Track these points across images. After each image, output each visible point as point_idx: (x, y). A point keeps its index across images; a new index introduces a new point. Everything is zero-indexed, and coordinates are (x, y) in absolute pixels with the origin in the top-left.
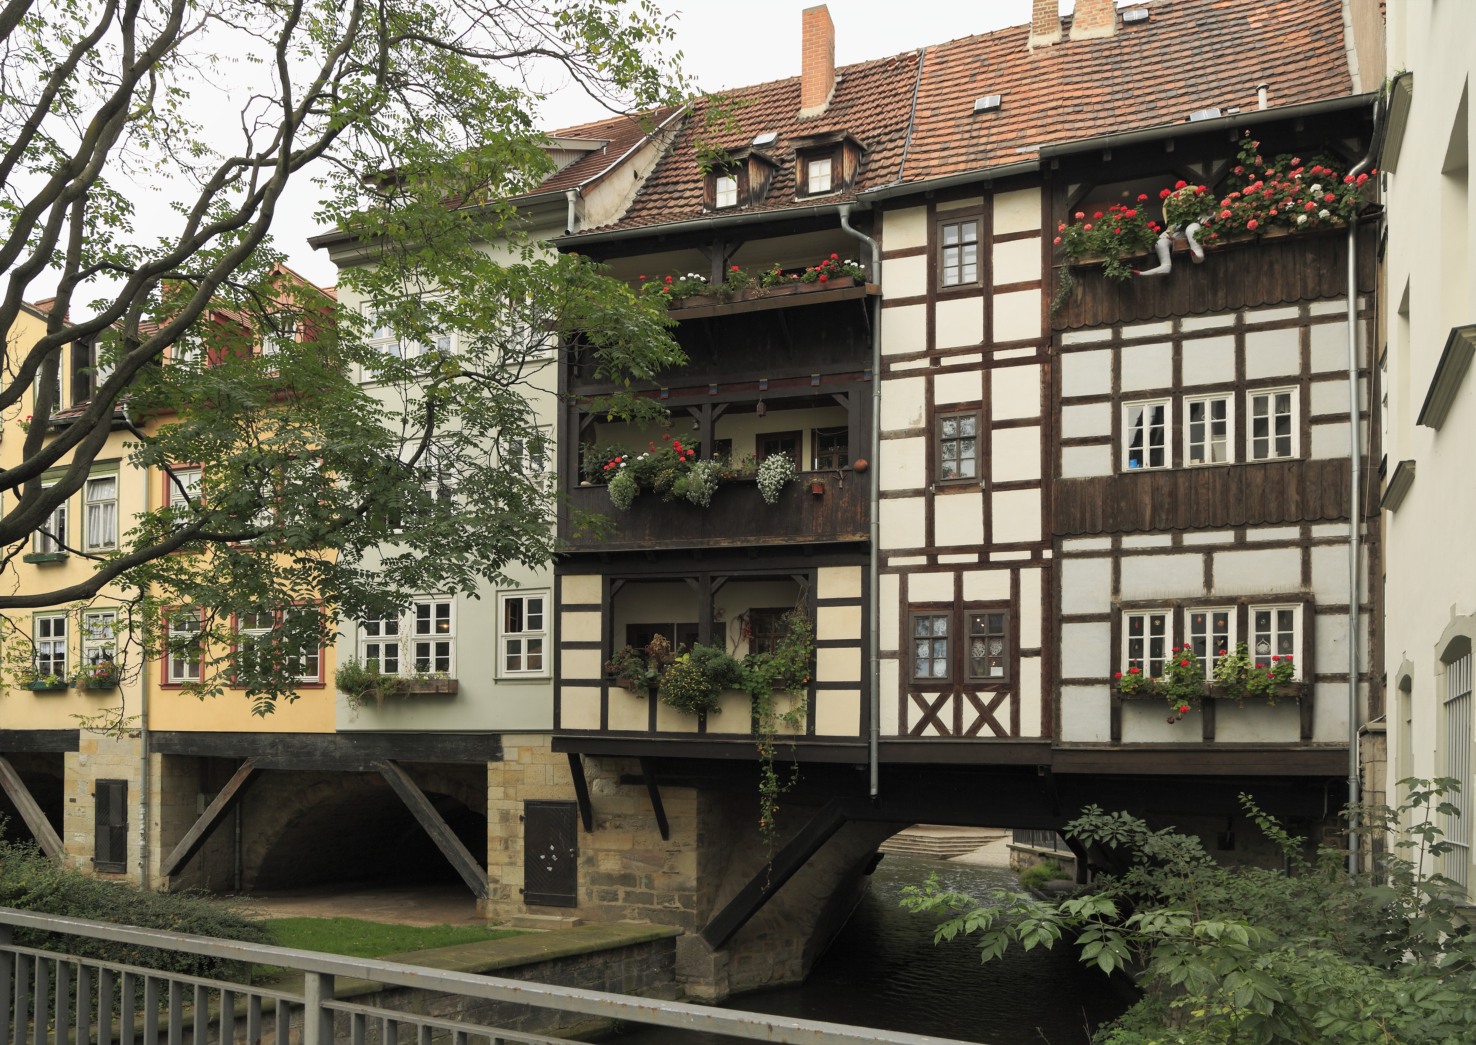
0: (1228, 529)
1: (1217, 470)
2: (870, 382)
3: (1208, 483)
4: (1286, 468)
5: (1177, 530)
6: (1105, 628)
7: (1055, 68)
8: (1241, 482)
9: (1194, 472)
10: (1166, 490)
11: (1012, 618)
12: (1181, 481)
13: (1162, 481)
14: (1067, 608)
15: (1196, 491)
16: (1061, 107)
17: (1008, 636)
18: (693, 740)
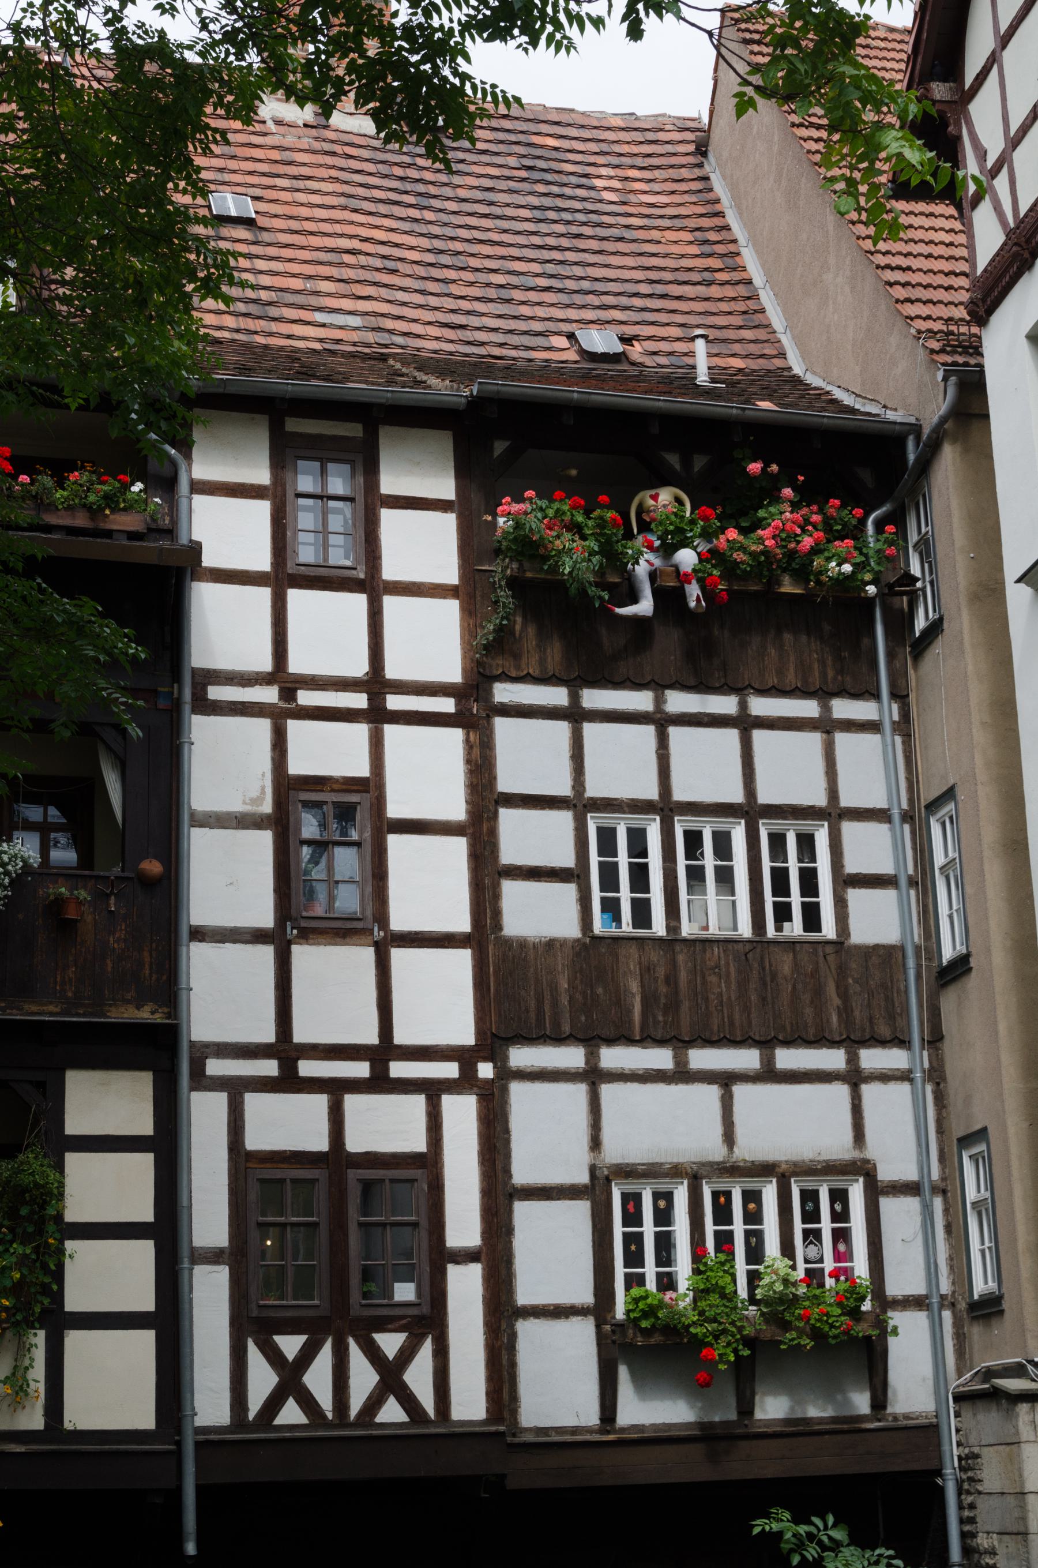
0: (750, 1047)
1: (730, 946)
3: (718, 966)
4: (820, 950)
5: (680, 1043)
6: (581, 1210)
7: (324, 173)
8: (764, 969)
9: (698, 945)
10: (661, 972)
12: (681, 958)
13: (654, 956)
14: (522, 1174)
15: (703, 977)
17: (424, 1223)
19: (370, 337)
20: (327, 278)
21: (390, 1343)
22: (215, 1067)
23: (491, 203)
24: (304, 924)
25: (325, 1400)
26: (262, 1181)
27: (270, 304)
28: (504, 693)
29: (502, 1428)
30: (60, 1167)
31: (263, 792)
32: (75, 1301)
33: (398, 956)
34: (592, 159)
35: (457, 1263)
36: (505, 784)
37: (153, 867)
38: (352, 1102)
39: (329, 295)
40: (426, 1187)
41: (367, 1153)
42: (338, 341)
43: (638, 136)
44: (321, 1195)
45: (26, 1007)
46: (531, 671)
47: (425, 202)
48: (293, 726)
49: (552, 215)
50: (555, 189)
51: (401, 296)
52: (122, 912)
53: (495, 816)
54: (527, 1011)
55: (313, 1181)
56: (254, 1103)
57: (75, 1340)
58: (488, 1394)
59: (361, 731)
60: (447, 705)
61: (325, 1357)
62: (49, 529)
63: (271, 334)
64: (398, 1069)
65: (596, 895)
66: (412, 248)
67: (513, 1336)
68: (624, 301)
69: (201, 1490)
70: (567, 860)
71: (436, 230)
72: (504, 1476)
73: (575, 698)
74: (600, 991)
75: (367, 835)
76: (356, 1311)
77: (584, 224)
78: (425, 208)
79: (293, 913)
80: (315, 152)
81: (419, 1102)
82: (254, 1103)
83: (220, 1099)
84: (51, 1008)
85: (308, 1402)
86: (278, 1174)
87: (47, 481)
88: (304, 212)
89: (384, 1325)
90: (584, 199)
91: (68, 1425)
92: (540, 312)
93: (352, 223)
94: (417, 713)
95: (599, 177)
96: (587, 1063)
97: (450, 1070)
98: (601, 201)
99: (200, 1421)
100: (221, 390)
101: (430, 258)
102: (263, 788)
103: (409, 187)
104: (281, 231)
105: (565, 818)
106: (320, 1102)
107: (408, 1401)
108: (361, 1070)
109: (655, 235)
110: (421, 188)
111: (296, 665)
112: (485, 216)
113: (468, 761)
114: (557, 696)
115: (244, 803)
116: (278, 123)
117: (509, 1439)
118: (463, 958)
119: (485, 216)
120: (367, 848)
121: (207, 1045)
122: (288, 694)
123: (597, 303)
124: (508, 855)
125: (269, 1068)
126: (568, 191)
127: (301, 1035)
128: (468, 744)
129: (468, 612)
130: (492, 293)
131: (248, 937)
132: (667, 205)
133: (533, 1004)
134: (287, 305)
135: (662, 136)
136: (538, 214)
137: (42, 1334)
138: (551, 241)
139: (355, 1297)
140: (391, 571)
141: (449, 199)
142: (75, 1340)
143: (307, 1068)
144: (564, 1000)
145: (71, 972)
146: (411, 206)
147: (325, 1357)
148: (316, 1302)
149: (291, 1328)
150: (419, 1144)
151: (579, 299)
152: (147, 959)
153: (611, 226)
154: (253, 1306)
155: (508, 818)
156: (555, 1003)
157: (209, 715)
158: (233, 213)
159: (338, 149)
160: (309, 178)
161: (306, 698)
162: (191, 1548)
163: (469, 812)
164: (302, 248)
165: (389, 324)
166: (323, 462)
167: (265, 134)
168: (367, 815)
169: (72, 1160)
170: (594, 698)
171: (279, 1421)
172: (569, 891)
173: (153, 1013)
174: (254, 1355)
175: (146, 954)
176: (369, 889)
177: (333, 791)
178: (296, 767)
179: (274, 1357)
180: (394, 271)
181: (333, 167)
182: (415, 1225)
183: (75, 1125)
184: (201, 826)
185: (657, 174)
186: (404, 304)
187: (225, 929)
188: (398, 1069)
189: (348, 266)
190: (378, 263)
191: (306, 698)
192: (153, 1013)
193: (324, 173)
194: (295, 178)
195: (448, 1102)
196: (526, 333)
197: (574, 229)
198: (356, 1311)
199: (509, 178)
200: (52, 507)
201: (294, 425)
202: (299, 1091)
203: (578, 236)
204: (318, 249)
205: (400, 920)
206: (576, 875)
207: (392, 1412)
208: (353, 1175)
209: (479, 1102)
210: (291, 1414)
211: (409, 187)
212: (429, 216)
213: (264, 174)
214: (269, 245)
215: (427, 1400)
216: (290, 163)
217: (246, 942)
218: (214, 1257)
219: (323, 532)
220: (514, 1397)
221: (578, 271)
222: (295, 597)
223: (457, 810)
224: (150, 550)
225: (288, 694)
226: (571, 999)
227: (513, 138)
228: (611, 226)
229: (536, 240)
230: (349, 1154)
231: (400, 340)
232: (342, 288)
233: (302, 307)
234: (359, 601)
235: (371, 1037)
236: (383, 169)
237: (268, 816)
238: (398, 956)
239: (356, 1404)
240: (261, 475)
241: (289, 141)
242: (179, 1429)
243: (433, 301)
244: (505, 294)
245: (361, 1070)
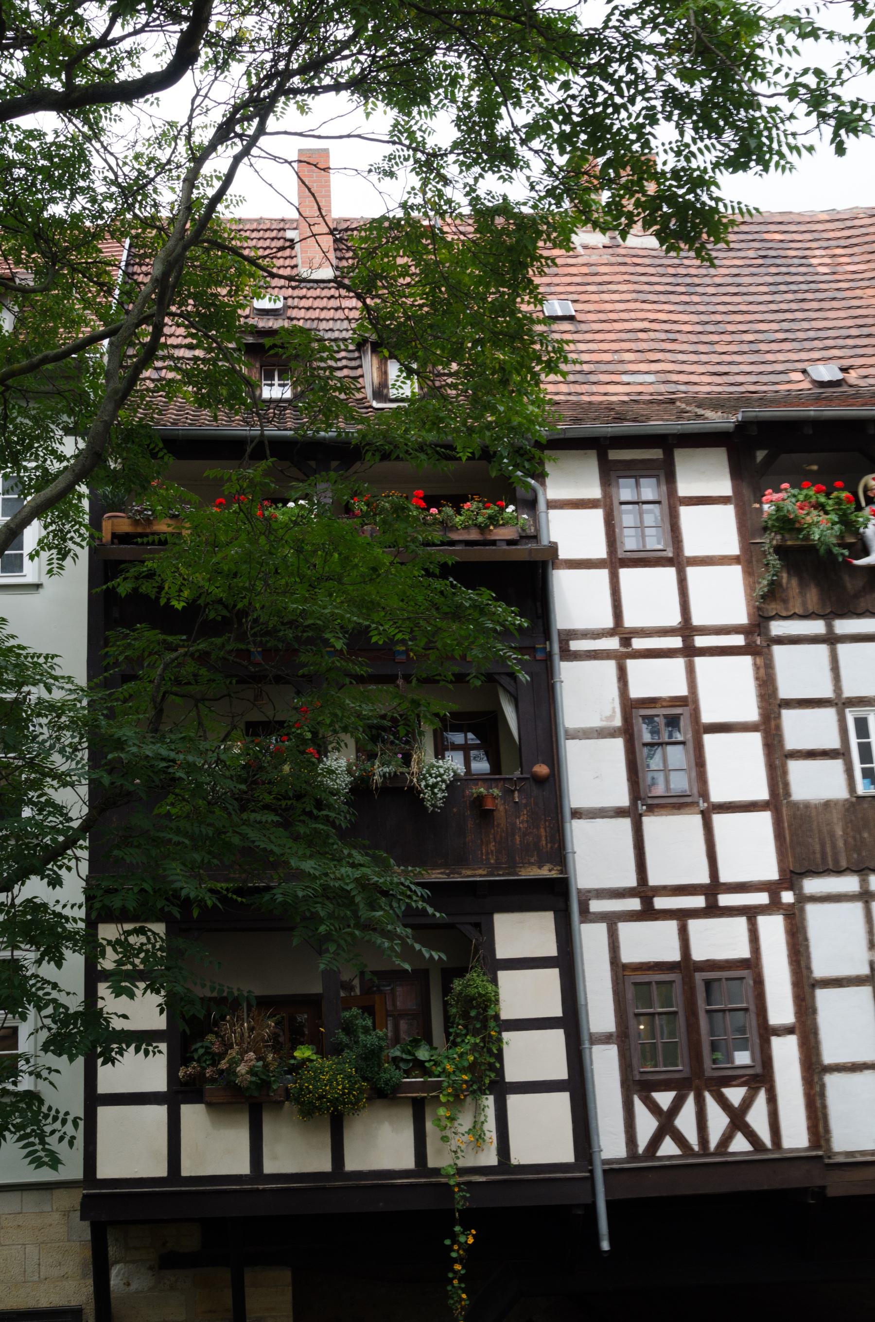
7: (620, 278)
11: (755, 982)
14: (820, 969)
16: (650, 330)
17: (752, 1008)
18: (328, 1184)
19: (662, 388)
20: (628, 351)
21: (735, 1095)
22: (596, 906)
23: (739, 285)
24: (650, 802)
25: (692, 1138)
26: (635, 984)
27: (591, 373)
28: (778, 628)
29: (820, 1153)
30: (495, 981)
31: (614, 711)
32: (511, 1076)
33: (718, 820)
34: (808, 245)
35: (778, 1035)
36: (785, 692)
37: (542, 769)
38: (693, 925)
39: (630, 362)
40: (751, 982)
41: (708, 961)
42: (640, 393)
43: (840, 225)
44: (677, 991)
45: (464, 872)
47: (692, 289)
48: (631, 664)
49: (783, 288)
50: (784, 270)
51: (681, 357)
53: (779, 716)
54: (814, 853)
55: (671, 983)
56: (625, 929)
57: (514, 1101)
58: (809, 1128)
59: (678, 664)
60: (739, 640)
61: (690, 1105)
62: (452, 543)
63: (593, 394)
64: (725, 900)
65: (858, 767)
66: (686, 323)
67: (823, 1086)
68: (841, 342)
69: (609, 1204)
70: (834, 743)
71: (702, 308)
72: (823, 1188)
73: (830, 627)
74: (866, 835)
75: (689, 736)
76: (709, 1073)
77: (807, 291)
78: (692, 294)
79: (642, 795)
80: (612, 264)
81: (741, 923)
82: (625, 929)
83: (601, 929)
84: (481, 872)
85: (680, 1139)
86: (646, 979)
87: (449, 510)
88: (609, 307)
89: (728, 1081)
90: (805, 274)
91: (514, 1162)
92: (781, 357)
93: (642, 310)
94: (717, 647)
95: (814, 257)
96: (861, 887)
97: (762, 898)
98: (817, 274)
99: (606, 1154)
100: (562, 436)
101: (699, 328)
102: (614, 709)
103: (679, 280)
104: (594, 322)
105: (829, 714)
106: (671, 927)
107: (751, 1136)
108: (699, 902)
109: (858, 293)
110: (688, 280)
112: (735, 294)
113: (757, 679)
114: (817, 627)
116: (585, 247)
117: (827, 1161)
118: (765, 818)
119: (735, 294)
120: (690, 745)
121: (589, 891)
122: (626, 641)
123: (821, 346)
124: (791, 742)
125: (634, 904)
126: (793, 270)
127: (654, 879)
128: (757, 667)
129: (748, 573)
130: (745, 347)
131: (612, 813)
132: (865, 271)
133: (817, 848)
134: (602, 373)
135: (857, 222)
136: (773, 288)
137: (491, 1098)
138: (784, 306)
139: (707, 1063)
140: (689, 550)
141: (708, 285)
142: (514, 1101)
143: (660, 903)
144: (840, 844)
145: (492, 847)
146: (682, 293)
147: (690, 1105)
148: (680, 1068)
149: (664, 1086)
150: (743, 952)
151: (808, 345)
152: (543, 834)
153: (826, 290)
154: (636, 1072)
155: (788, 717)
156: (834, 846)
158: (560, 313)
159: (628, 260)
160: (610, 283)
161: (638, 644)
162: (605, 1246)
163: (761, 715)
164: (609, 332)
165: (675, 377)
166: (637, 478)
167: (577, 257)
168: (688, 722)
169: (502, 975)
170: (843, 626)
171: (660, 1153)
172: (838, 765)
173: (550, 870)
174: (639, 1106)
175: (542, 830)
176: (694, 774)
177: (663, 707)
178: (635, 693)
179: (654, 1108)
180: (674, 341)
181: (625, 273)
182: (746, 1010)
183: (502, 952)
185: (856, 250)
186: (684, 362)
187: (595, 809)
188: (725, 900)
189: (642, 340)
190: (663, 336)
191: (638, 644)
192: (550, 870)
193: (620, 278)
194: (600, 284)
195: (763, 921)
196: (772, 373)
197: (800, 296)
198: (709, 1073)
199: (750, 266)
200: (453, 528)
201: (615, 455)
202: (656, 919)
203: (803, 300)
204: (620, 331)
205: (717, 795)
206: (841, 753)
207: (740, 1144)
208: (699, 977)
209: (785, 920)
210: (668, 1148)
211: (679, 280)
212: (696, 299)
213: (578, 284)
214: (586, 332)
215: (765, 1135)
216: (596, 274)
218: (606, 1039)
219: (641, 527)
220: (827, 1130)
221: (805, 325)
222: (626, 574)
223: (752, 714)
224: (522, 552)
225: (626, 641)
226: (846, 843)
227: (750, 237)
228: (826, 290)
229: (773, 307)
230: (695, 962)
231: (683, 388)
232: (639, 356)
233: (612, 373)
234: (670, 573)
235: (704, 878)
236: (661, 270)
237: (619, 728)
238: (718, 820)
239: (714, 1140)
240: (595, 492)
241: (594, 259)
242: (591, 1162)
243: (704, 358)
244: (754, 347)
245: (699, 902)
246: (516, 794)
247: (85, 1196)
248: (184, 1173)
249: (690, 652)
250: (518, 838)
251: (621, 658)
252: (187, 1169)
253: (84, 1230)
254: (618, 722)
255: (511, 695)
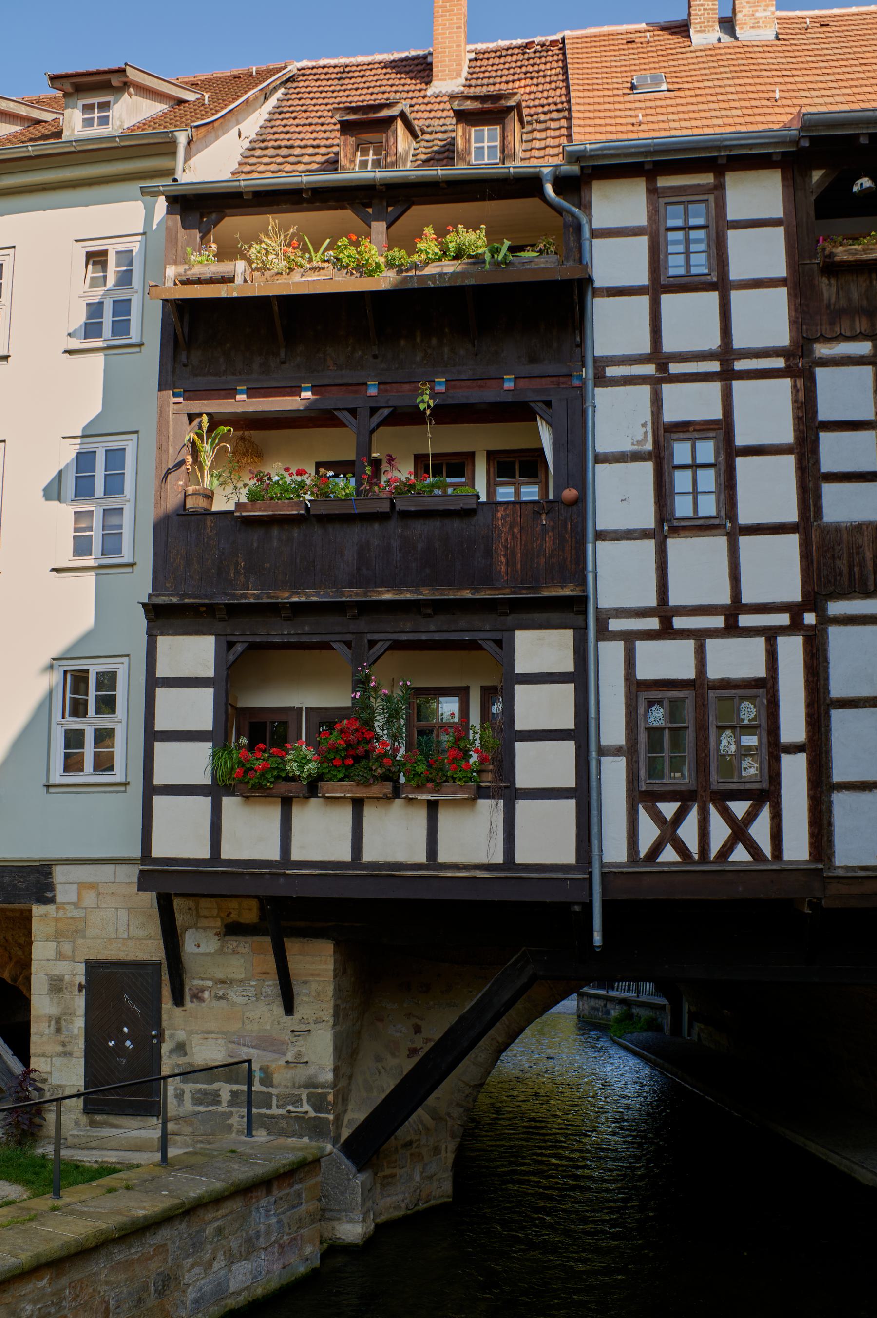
2: (582, 388)
28: (822, 350)
36: (824, 415)
46: (843, 332)
52: (552, 523)
59: (715, 387)
60: (779, 363)
94: (756, 370)
111: (669, 345)
113: (795, 401)
115: (633, 444)
122: (662, 367)
128: (795, 389)
140: (735, 273)
157: (607, 387)
161: (675, 368)
176: (723, 497)
178: (669, 416)
183: (519, 668)
184: (603, 462)
191: (675, 368)
201: (663, 182)
217: (635, 539)
223: (787, 436)
225: (662, 367)
237: (650, 453)
246: (544, 516)
247: (141, 871)
248: (224, 856)
249: (727, 375)
250: (543, 560)
251: (656, 383)
252: (227, 853)
253: (149, 898)
254: (649, 446)
255: (547, 423)
